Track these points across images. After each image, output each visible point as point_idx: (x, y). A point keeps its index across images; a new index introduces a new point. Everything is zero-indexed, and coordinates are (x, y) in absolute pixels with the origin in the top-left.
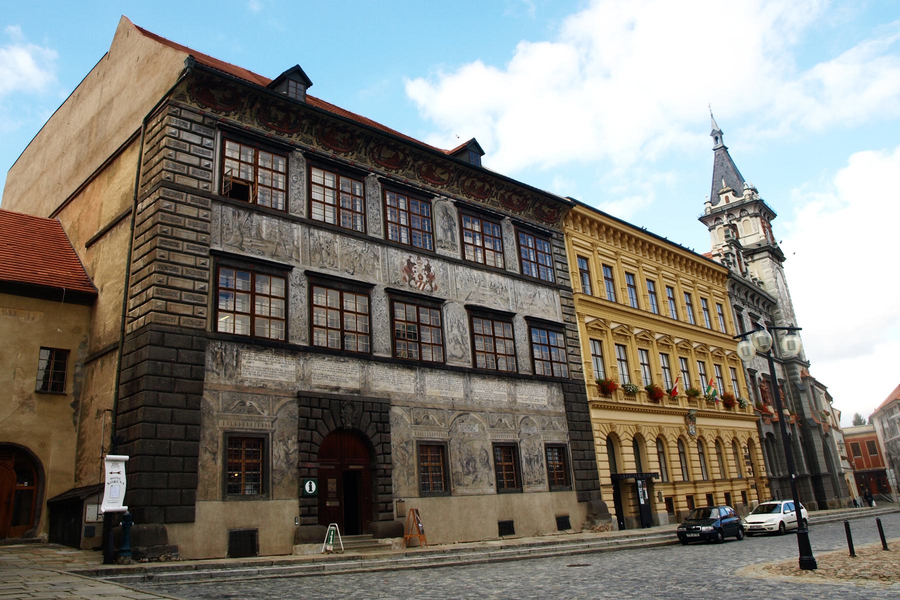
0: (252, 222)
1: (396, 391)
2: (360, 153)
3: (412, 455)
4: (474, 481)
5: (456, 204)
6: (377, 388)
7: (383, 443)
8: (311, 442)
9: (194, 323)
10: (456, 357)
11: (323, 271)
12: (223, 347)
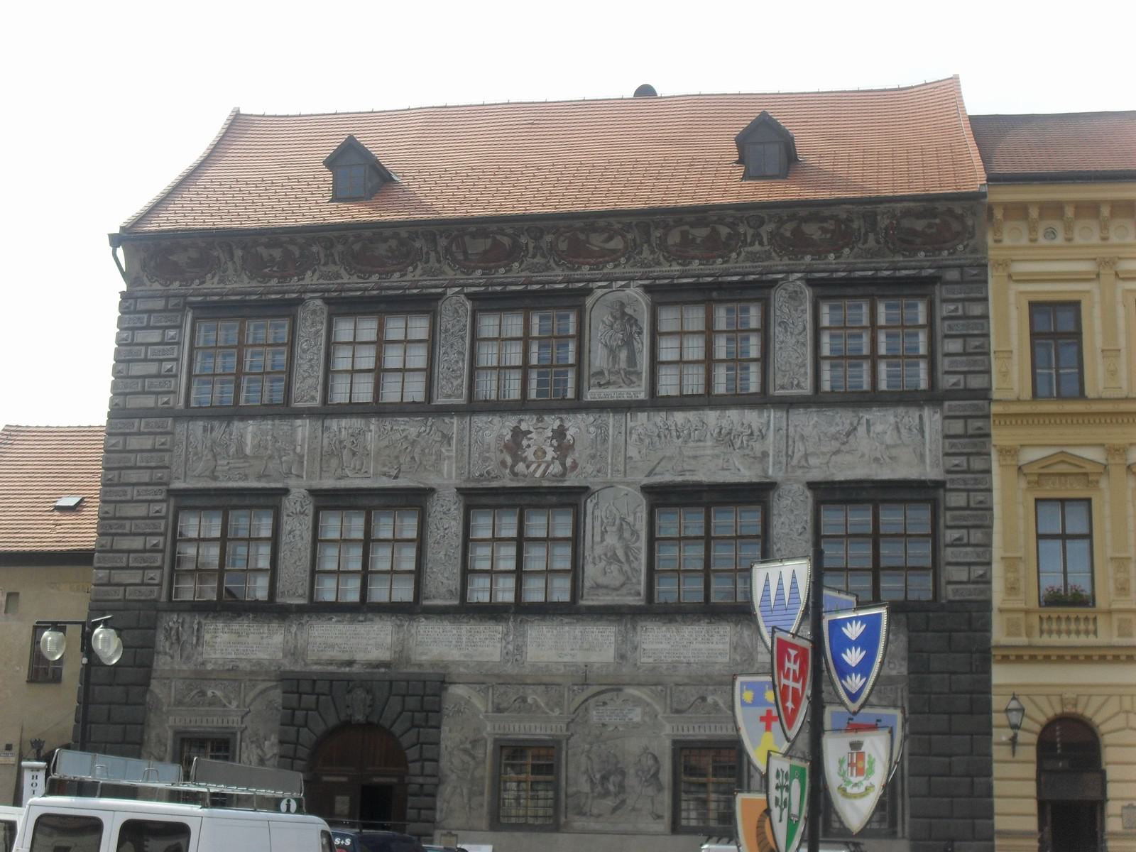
0: (231, 435)
1: (462, 658)
2: (427, 262)
3: (484, 762)
4: (615, 809)
5: (648, 289)
6: (424, 658)
7: (422, 744)
8: (297, 743)
9: (145, 593)
10: (606, 587)
11: (342, 484)
12: (180, 621)
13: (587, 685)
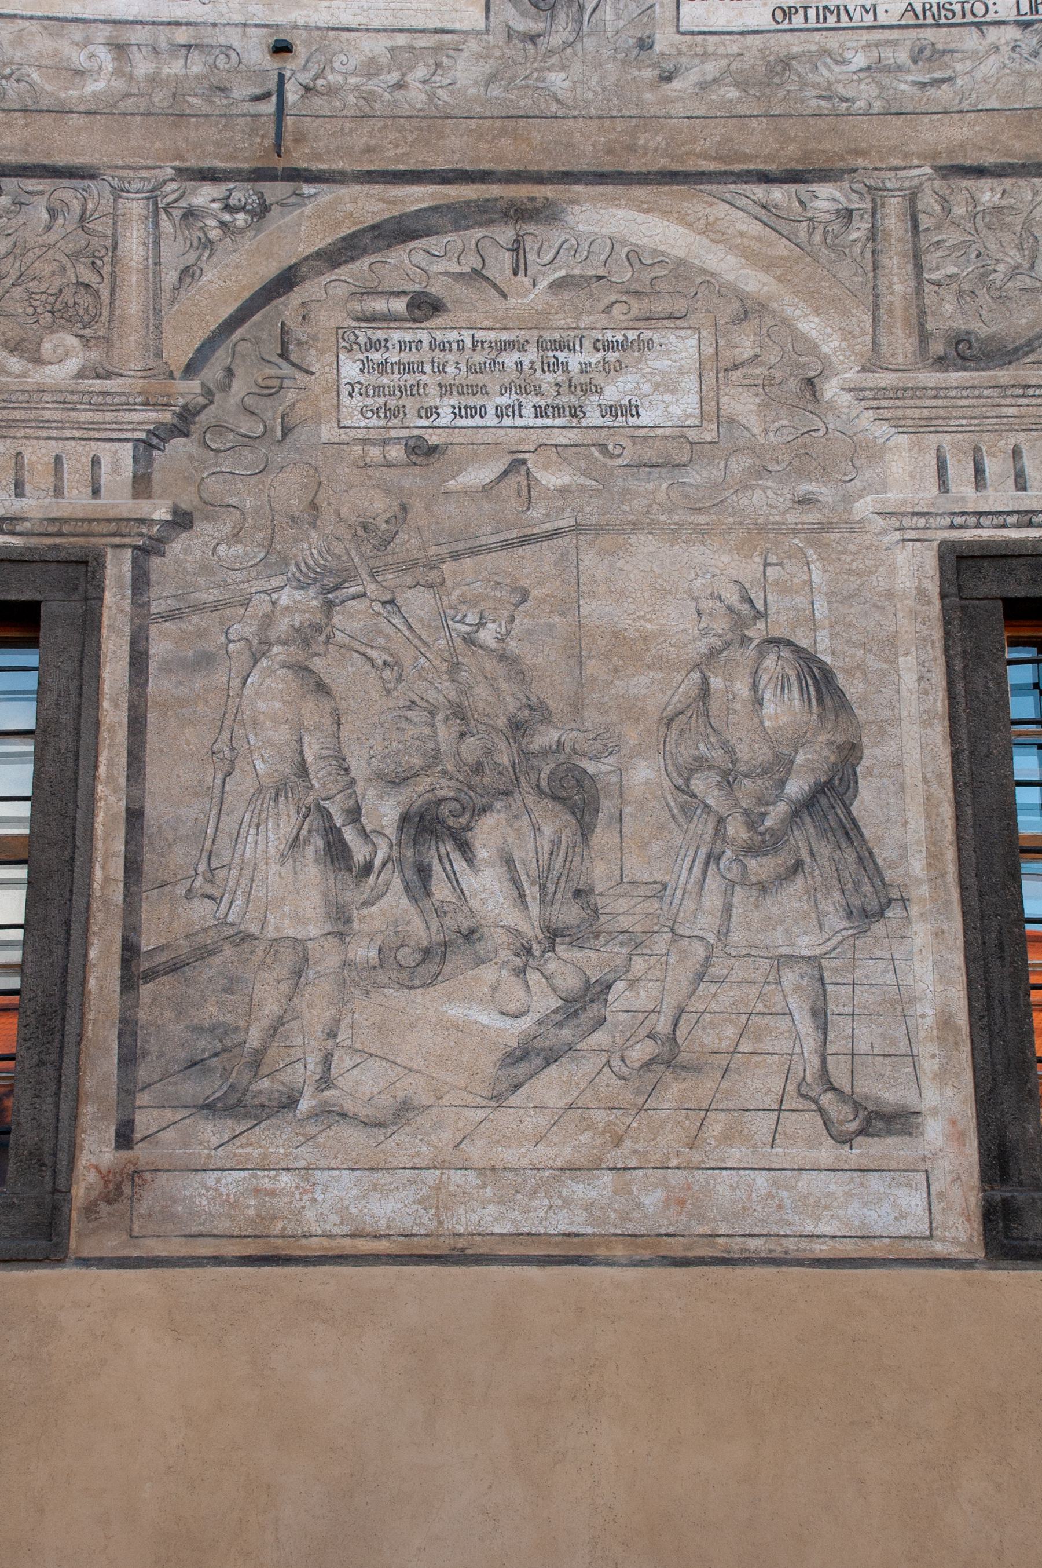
13: (296, 175)
